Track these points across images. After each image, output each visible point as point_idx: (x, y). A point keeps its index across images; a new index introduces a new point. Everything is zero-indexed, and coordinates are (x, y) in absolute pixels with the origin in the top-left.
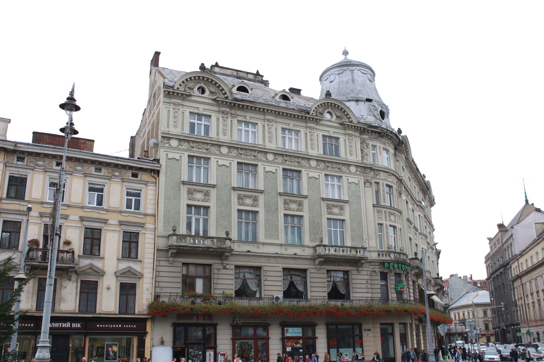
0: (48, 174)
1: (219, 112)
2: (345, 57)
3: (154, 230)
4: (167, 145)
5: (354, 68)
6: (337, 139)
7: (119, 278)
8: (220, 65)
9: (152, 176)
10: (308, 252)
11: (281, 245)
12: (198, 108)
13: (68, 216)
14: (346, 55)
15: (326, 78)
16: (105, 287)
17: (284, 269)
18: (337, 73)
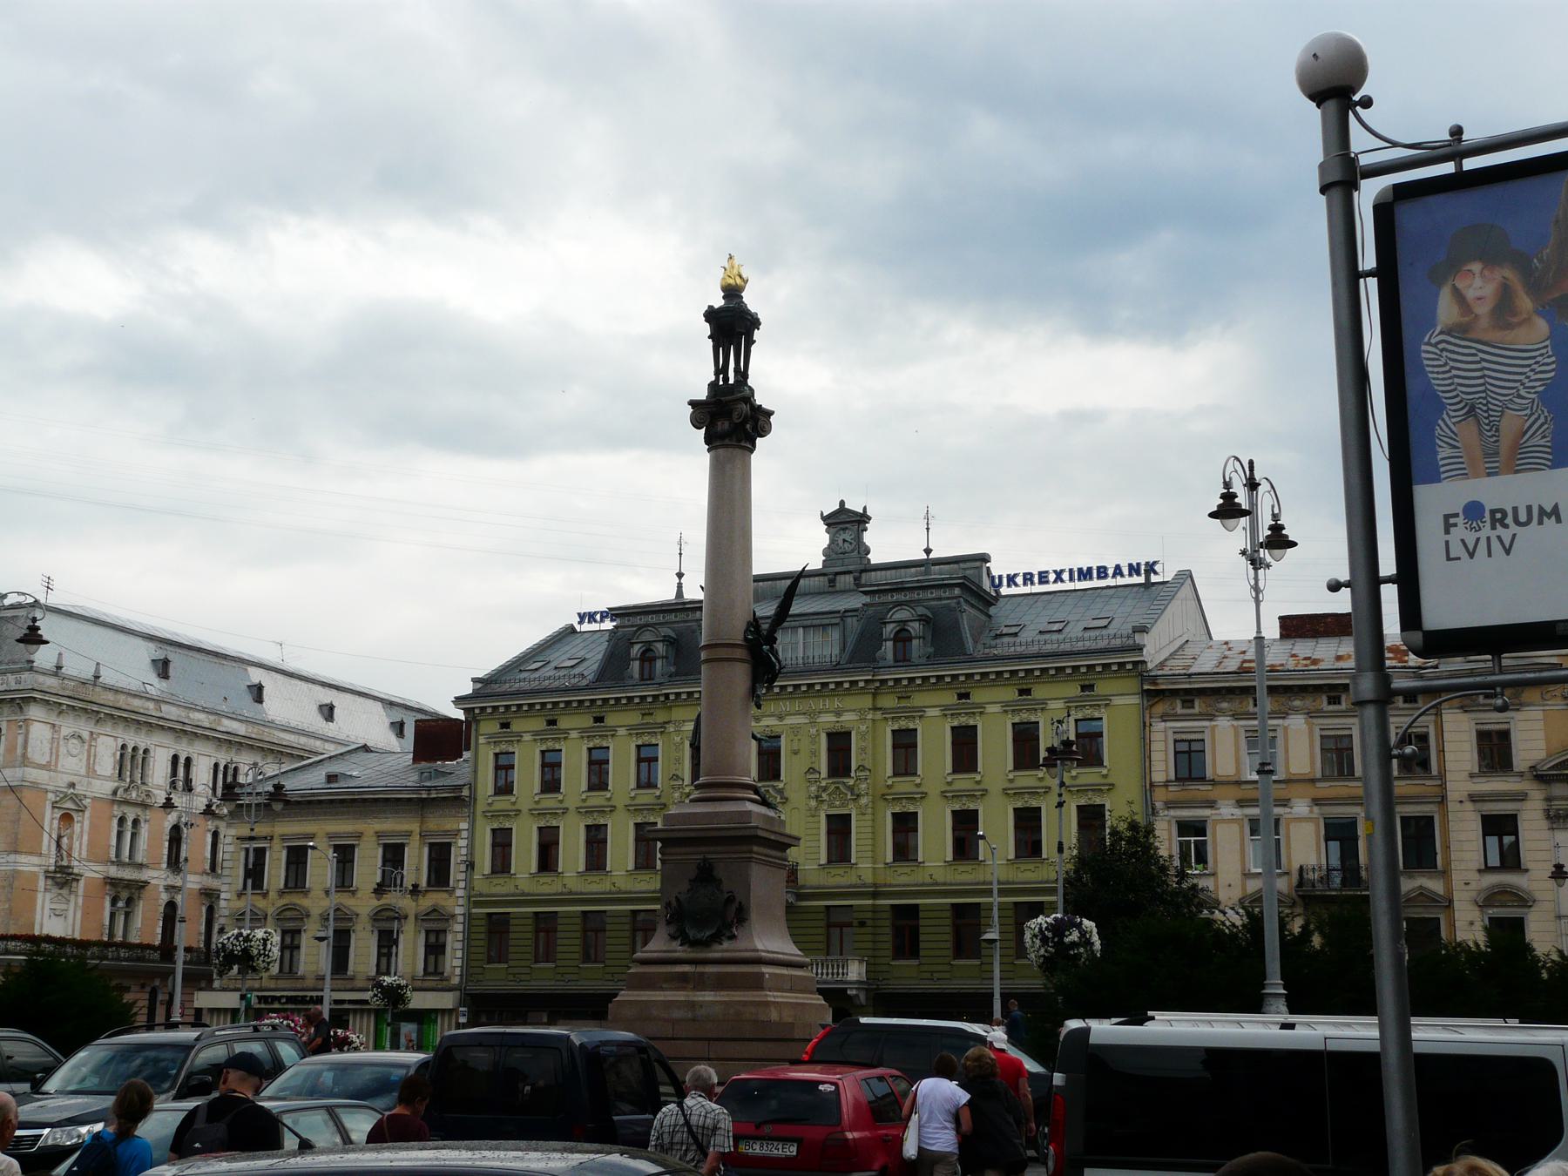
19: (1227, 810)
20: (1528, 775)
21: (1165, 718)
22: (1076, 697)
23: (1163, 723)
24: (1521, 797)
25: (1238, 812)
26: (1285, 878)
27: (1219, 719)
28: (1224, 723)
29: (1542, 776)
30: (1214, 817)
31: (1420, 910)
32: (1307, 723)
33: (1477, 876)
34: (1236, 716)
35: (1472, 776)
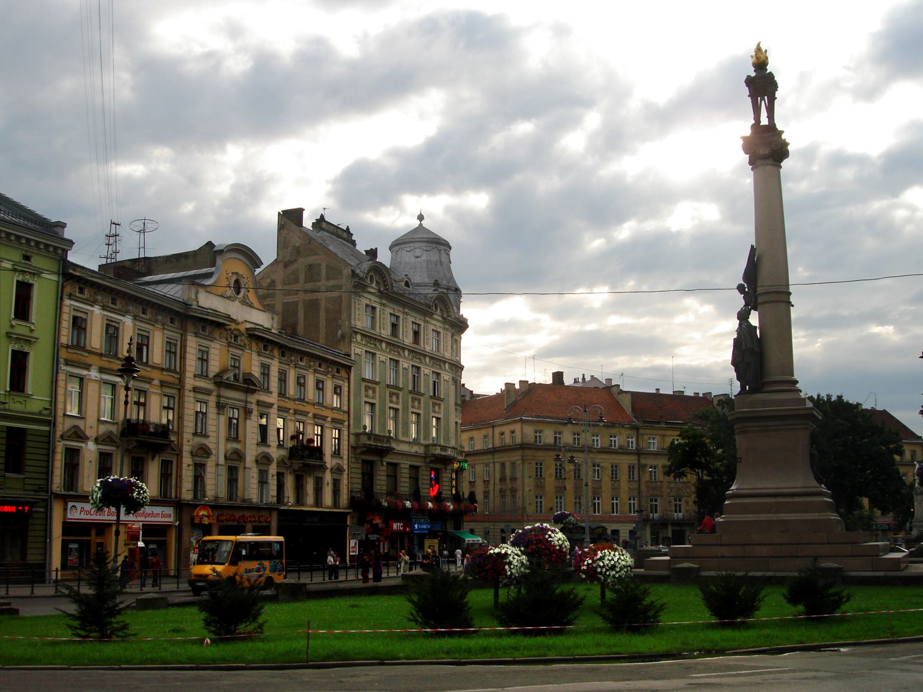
0: (297, 369)
1: (381, 304)
2: (419, 222)
3: (347, 427)
4: (355, 340)
5: (442, 247)
6: (440, 332)
7: (334, 475)
8: (326, 220)
9: (347, 372)
10: (421, 450)
11: (409, 443)
12: (370, 300)
13: (309, 413)
14: (421, 221)
15: (409, 249)
16: (326, 482)
17: (411, 466)
18: (424, 248)
19: (94, 374)
20: (213, 381)
21: (70, 297)
22: (20, 262)
23: (69, 301)
24: (208, 392)
25: (98, 375)
26: (116, 426)
27: (96, 306)
28: (97, 310)
29: (221, 382)
30: (87, 377)
31: (167, 455)
32: (132, 322)
33: (190, 437)
34: (104, 308)
35: (195, 376)
